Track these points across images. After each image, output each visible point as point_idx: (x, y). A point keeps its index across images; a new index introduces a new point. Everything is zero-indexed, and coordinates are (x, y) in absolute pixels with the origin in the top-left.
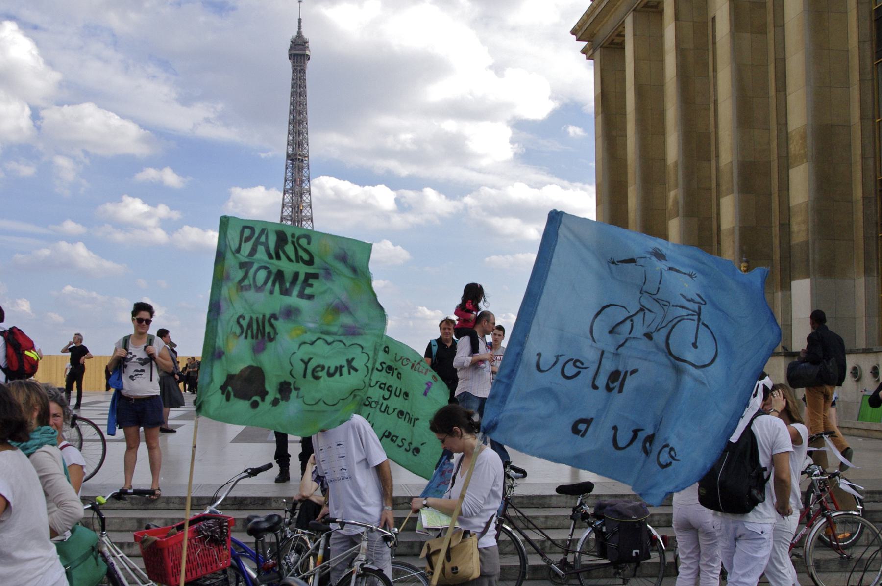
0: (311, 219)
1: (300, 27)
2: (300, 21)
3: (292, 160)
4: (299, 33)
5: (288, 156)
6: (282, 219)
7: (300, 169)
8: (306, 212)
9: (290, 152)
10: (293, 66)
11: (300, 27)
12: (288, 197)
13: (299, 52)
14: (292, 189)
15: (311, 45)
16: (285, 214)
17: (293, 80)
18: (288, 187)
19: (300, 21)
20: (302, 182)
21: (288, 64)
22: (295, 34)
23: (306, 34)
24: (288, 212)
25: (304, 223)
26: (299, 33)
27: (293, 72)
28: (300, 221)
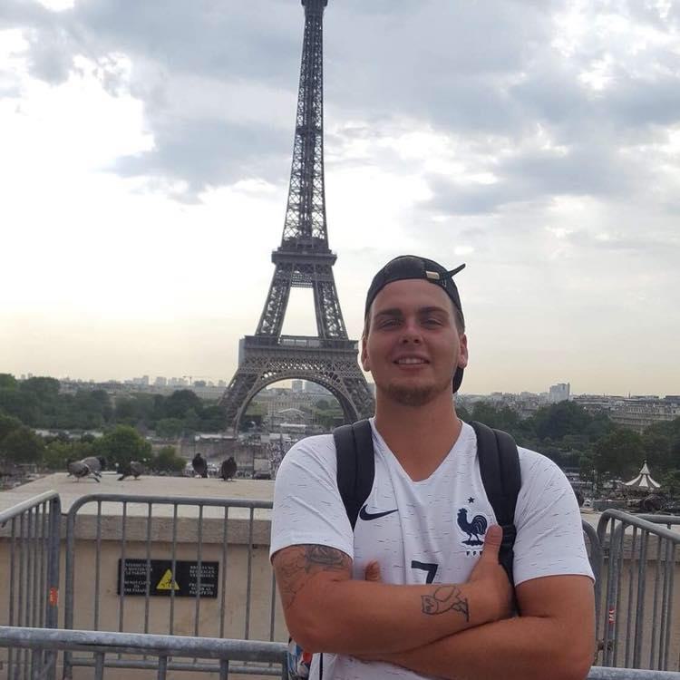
0: (323, 210)
5: (299, 130)
6: (289, 207)
7: (313, 145)
8: (317, 200)
9: (301, 124)
10: (307, 13)
12: (297, 183)
14: (300, 171)
16: (292, 202)
17: (306, 30)
18: (296, 168)
20: (314, 162)
24: (296, 199)
25: (314, 214)
27: (307, 22)
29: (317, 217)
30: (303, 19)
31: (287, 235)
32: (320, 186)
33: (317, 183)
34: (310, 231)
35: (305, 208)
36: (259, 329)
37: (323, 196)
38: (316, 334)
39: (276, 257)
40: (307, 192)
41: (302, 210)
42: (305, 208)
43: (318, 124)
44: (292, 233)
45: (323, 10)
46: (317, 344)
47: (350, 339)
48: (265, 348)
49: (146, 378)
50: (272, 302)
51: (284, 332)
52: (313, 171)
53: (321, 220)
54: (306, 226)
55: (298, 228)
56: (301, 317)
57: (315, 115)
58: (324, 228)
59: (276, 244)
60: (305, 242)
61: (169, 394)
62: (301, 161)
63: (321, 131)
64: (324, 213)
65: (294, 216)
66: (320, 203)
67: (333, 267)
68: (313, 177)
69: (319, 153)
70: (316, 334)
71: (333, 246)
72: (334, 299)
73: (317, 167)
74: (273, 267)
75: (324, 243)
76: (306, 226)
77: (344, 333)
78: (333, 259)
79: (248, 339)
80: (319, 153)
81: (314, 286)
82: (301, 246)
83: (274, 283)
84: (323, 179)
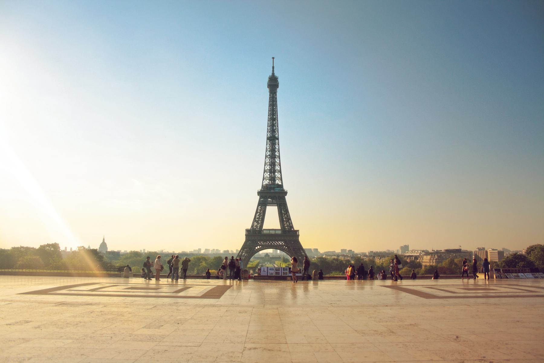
0: (280, 171)
1: (273, 71)
2: (273, 67)
3: (270, 140)
4: (273, 74)
5: (268, 139)
6: (265, 171)
8: (277, 168)
11: (273, 71)
12: (268, 160)
13: (273, 84)
14: (269, 155)
15: (279, 80)
19: (273, 67)
20: (275, 152)
21: (267, 90)
22: (271, 74)
23: (276, 74)
24: (268, 168)
25: (276, 174)
26: (273, 74)
28: (274, 172)
29: (277, 175)
30: (269, 94)
31: (264, 183)
32: (278, 161)
33: (277, 160)
34: (275, 181)
35: (272, 171)
36: (252, 226)
37: (280, 165)
38: (280, 228)
39: (259, 193)
40: (273, 164)
41: (271, 172)
42: (272, 171)
43: (277, 136)
44: (266, 182)
45: (276, 90)
46: (280, 232)
47: (295, 229)
48: (256, 237)
49: (200, 250)
50: (258, 214)
51: (265, 227)
52: (275, 155)
53: (279, 176)
54: (273, 179)
55: (269, 180)
56: (272, 221)
57: (275, 132)
58: (281, 180)
59: (259, 188)
60: (273, 186)
61: (212, 257)
62: (270, 151)
63: (278, 139)
64: (281, 173)
65: (267, 175)
66: (279, 169)
67: (287, 197)
68: (275, 157)
69: (277, 148)
70: (280, 228)
71: (285, 188)
72: (287, 211)
73: (277, 154)
74: (258, 197)
75: (281, 186)
76: (273, 179)
77: (292, 227)
78: (286, 193)
79: (247, 231)
80: (277, 148)
81: (277, 206)
82: (271, 188)
83: (260, 204)
84: (279, 158)
